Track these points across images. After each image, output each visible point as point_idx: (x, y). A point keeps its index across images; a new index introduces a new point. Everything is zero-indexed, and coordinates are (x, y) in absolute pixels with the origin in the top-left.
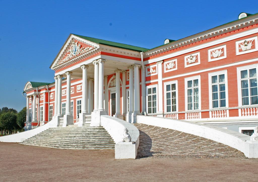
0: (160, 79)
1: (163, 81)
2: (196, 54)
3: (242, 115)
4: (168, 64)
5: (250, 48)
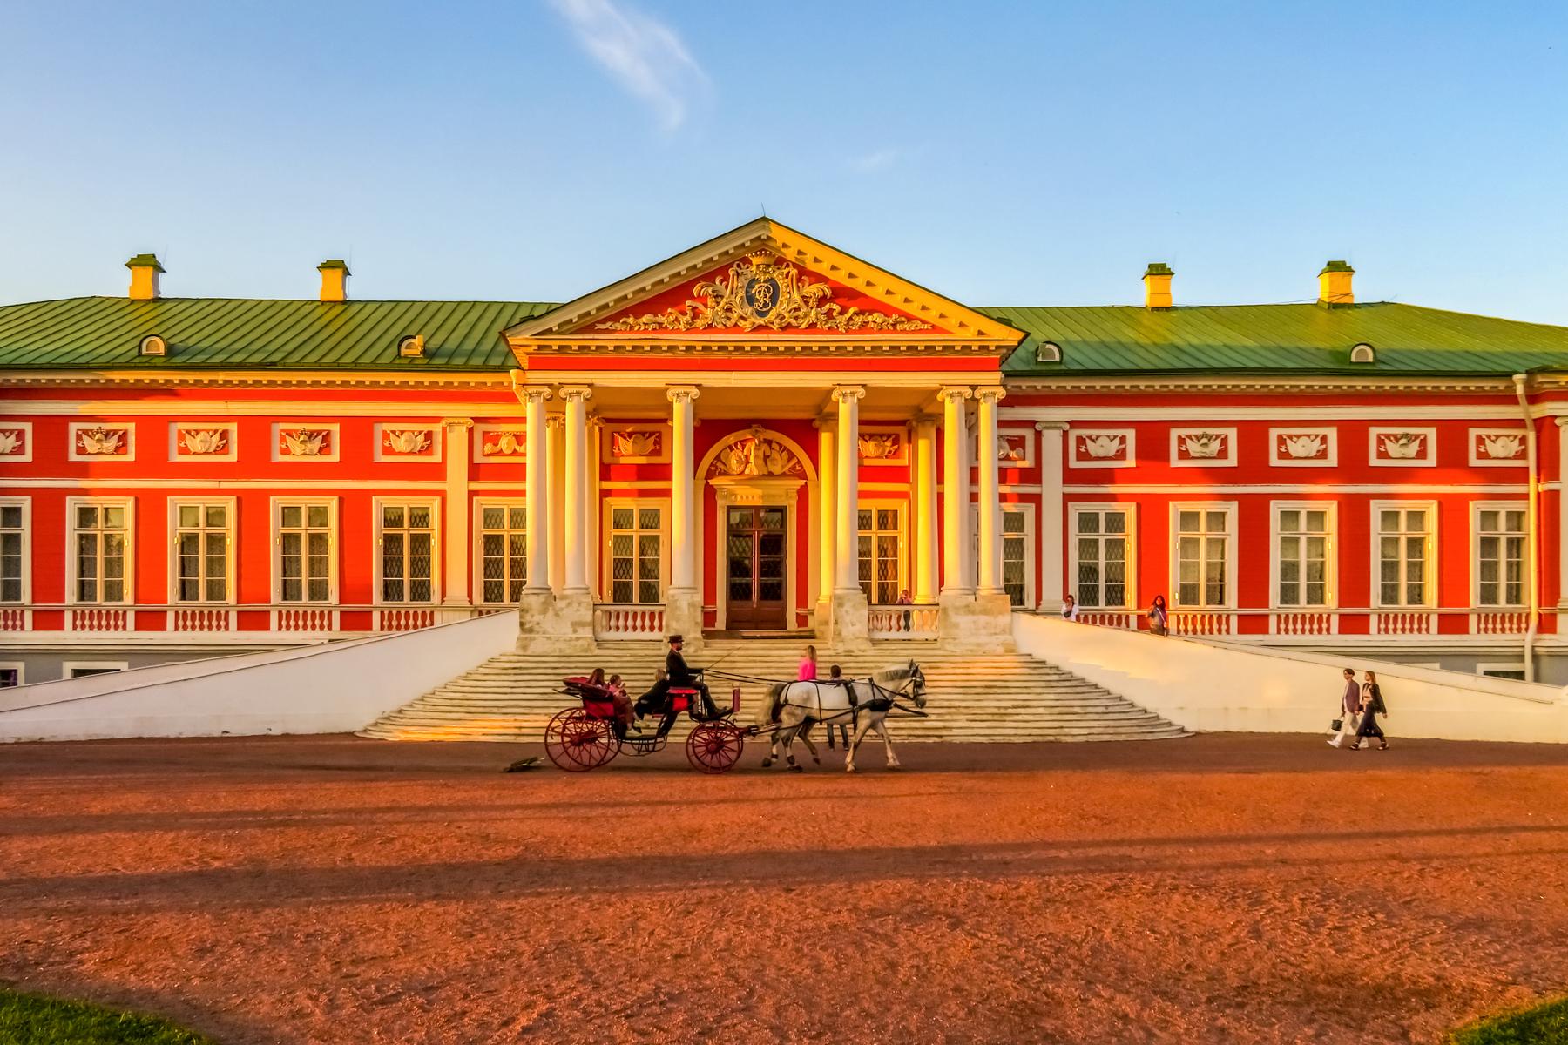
0: (1052, 487)
1: (1067, 498)
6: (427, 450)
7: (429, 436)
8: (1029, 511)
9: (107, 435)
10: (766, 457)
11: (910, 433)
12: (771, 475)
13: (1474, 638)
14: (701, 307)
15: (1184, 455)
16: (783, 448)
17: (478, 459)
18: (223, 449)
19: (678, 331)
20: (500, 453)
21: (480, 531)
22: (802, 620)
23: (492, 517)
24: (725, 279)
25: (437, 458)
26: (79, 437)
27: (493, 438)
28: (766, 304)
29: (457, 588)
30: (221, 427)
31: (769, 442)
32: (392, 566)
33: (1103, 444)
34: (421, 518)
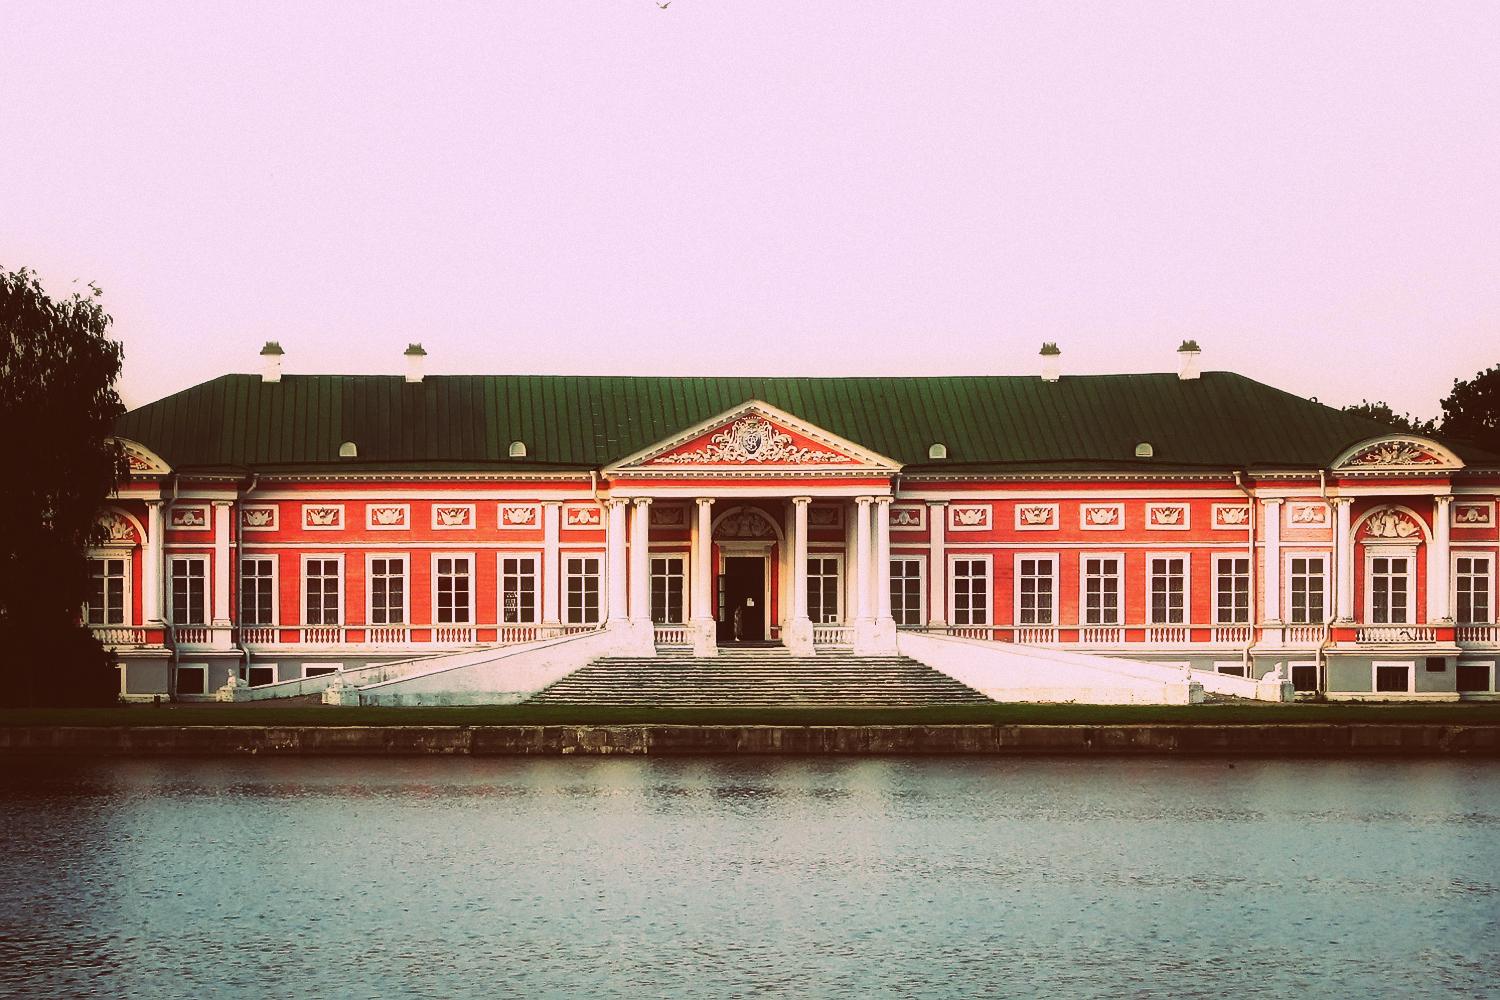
0: (938, 544)
2: (1049, 506)
3: (1086, 640)
4: (965, 512)
5: (1174, 521)
6: (531, 522)
7: (532, 511)
8: (922, 560)
9: (327, 513)
10: (750, 525)
11: (844, 508)
12: (754, 538)
13: (1213, 645)
14: (717, 449)
15: (1024, 521)
16: (762, 519)
17: (565, 526)
18: (401, 522)
19: (702, 464)
20: (579, 523)
21: (566, 576)
22: (774, 634)
23: (574, 566)
24: (730, 432)
25: (538, 526)
26: (309, 514)
27: (574, 513)
28: (753, 447)
29: (551, 614)
30: (399, 506)
31: (753, 515)
33: (971, 517)
34: (528, 565)
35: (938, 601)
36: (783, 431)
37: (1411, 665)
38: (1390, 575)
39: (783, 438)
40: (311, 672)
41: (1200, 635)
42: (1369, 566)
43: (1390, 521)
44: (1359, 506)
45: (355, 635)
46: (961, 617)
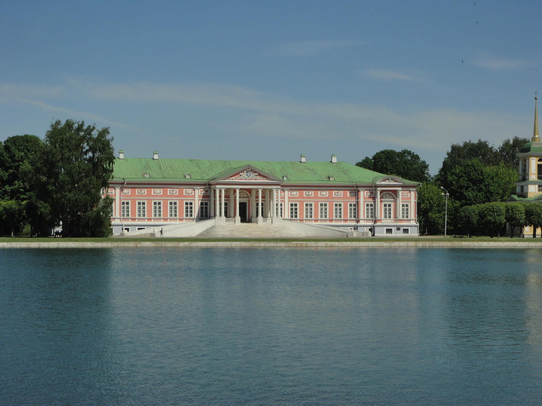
0: (286, 199)
6: (192, 193)
32: (187, 212)
34: (191, 204)
35: (287, 214)
36: (256, 172)
37: (393, 228)
38: (387, 207)
39: (257, 174)
40: (139, 229)
41: (345, 220)
42: (383, 205)
43: (387, 195)
44: (382, 192)
45: (149, 219)
46: (292, 216)
